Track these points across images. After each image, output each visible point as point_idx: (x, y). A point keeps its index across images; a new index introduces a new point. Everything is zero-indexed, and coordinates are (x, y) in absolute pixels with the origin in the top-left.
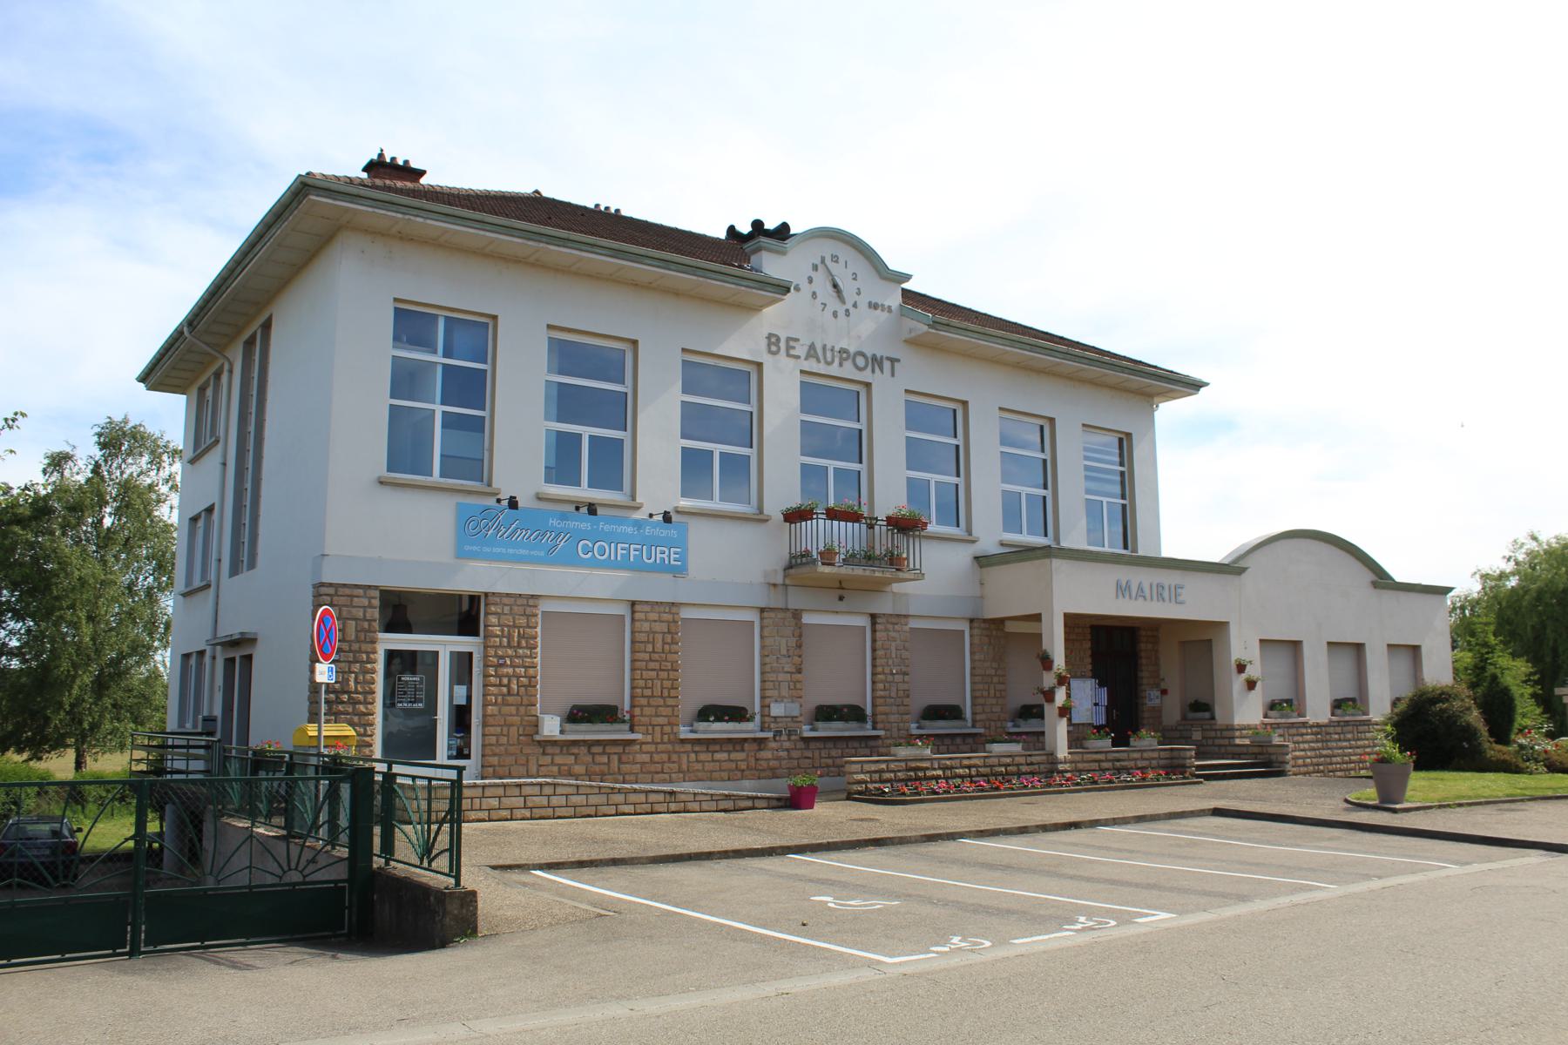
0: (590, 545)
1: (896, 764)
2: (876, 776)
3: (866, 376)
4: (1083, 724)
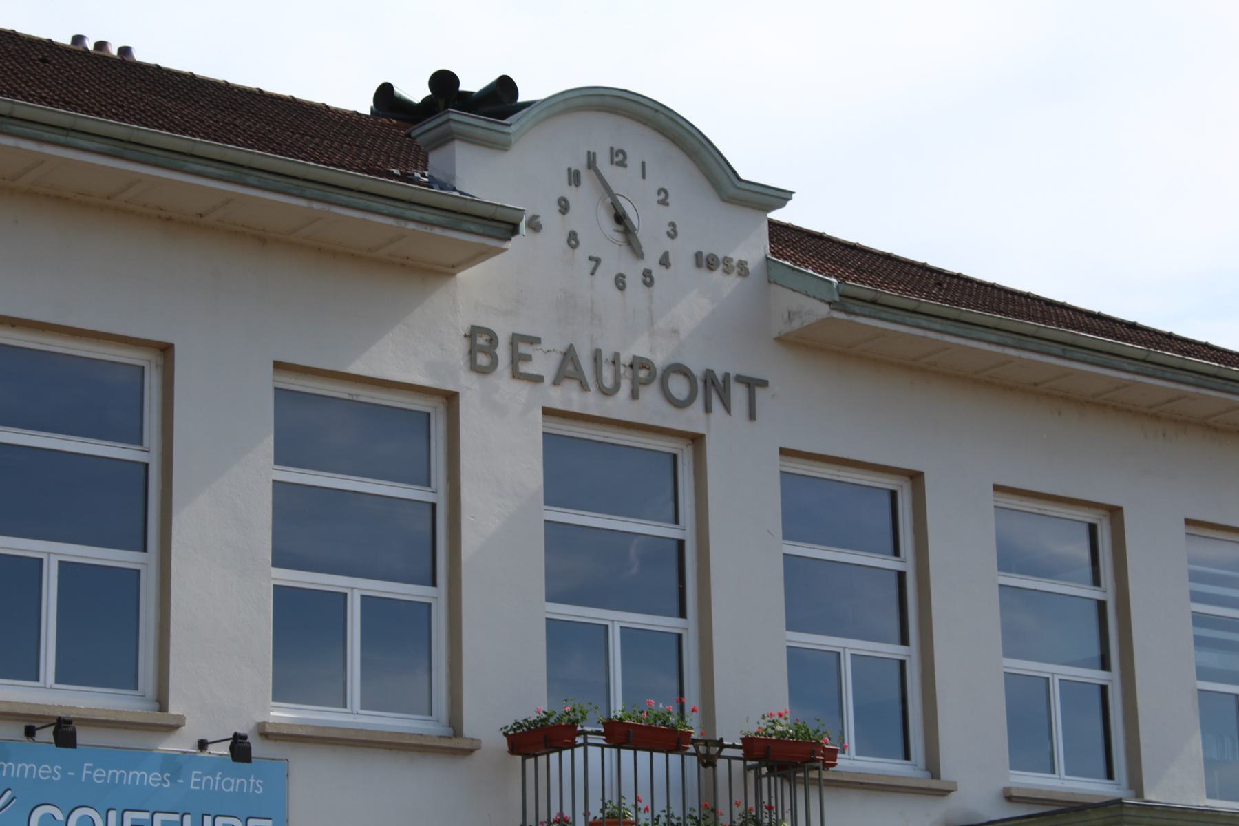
0: (60, 816)
3: (692, 419)
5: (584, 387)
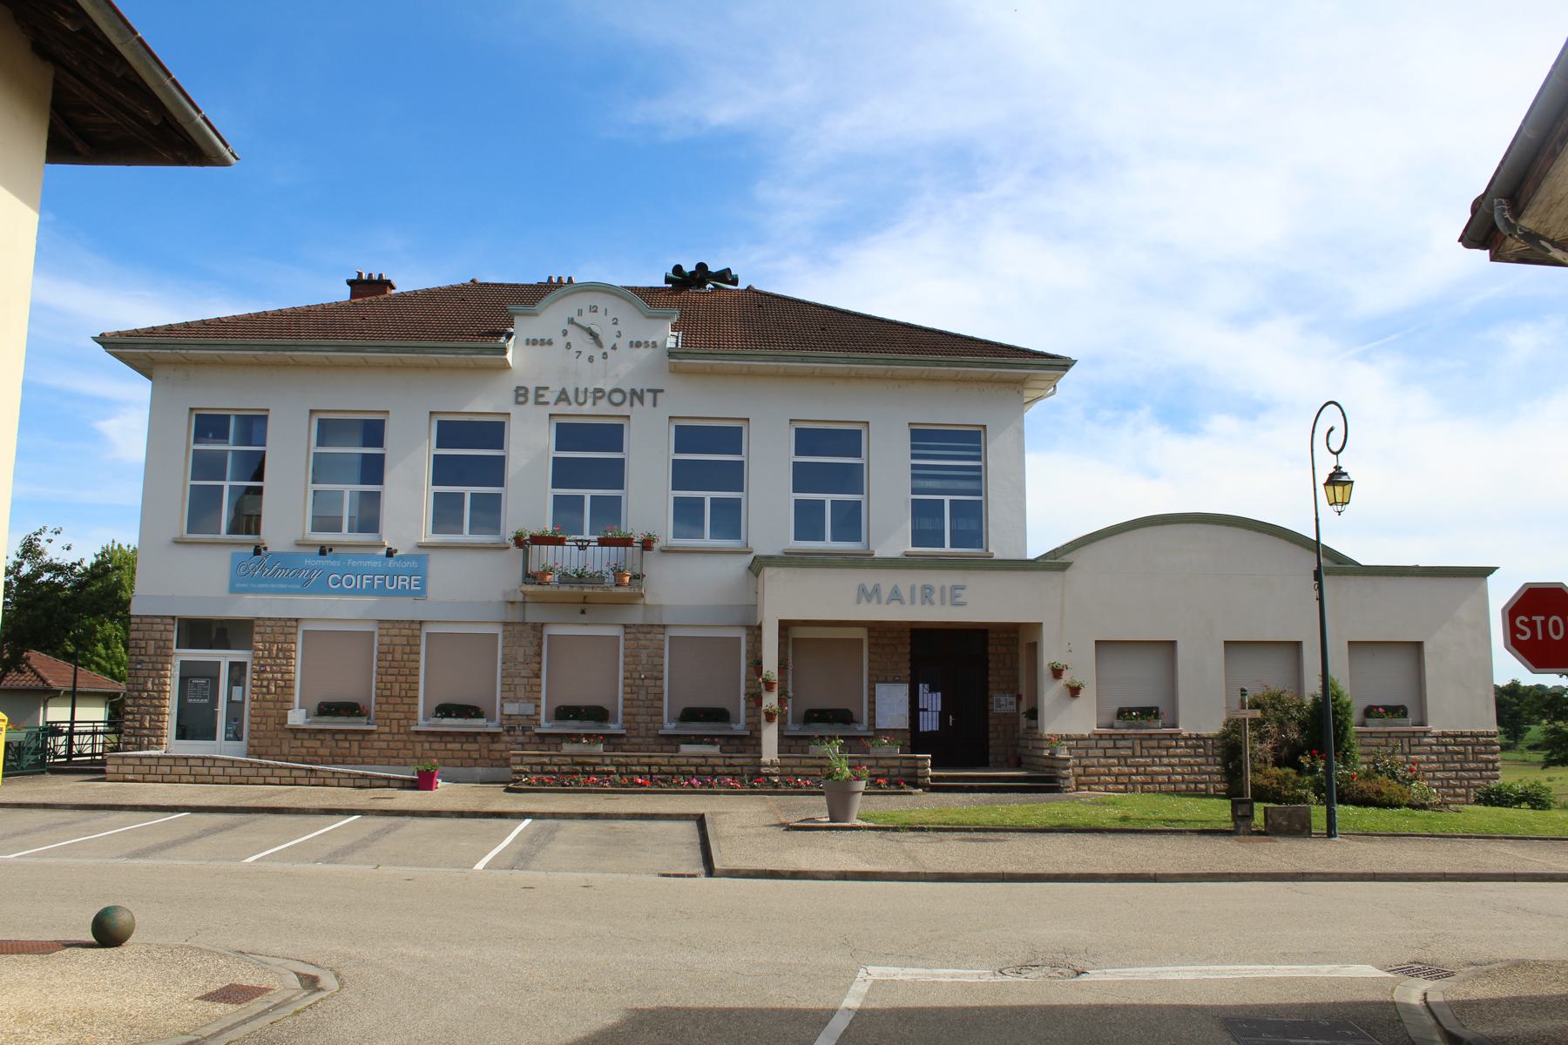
0: (339, 578)
1: (560, 758)
2: (538, 768)
3: (625, 409)
4: (894, 730)
5: (570, 404)
